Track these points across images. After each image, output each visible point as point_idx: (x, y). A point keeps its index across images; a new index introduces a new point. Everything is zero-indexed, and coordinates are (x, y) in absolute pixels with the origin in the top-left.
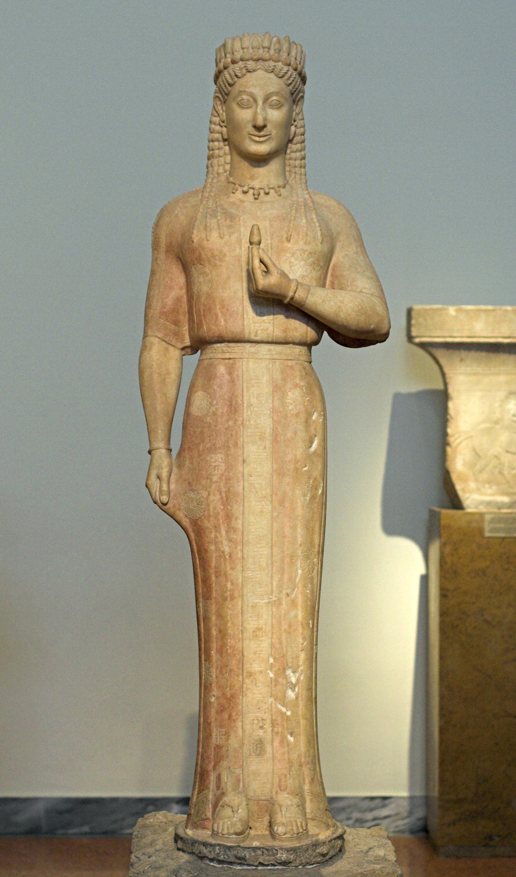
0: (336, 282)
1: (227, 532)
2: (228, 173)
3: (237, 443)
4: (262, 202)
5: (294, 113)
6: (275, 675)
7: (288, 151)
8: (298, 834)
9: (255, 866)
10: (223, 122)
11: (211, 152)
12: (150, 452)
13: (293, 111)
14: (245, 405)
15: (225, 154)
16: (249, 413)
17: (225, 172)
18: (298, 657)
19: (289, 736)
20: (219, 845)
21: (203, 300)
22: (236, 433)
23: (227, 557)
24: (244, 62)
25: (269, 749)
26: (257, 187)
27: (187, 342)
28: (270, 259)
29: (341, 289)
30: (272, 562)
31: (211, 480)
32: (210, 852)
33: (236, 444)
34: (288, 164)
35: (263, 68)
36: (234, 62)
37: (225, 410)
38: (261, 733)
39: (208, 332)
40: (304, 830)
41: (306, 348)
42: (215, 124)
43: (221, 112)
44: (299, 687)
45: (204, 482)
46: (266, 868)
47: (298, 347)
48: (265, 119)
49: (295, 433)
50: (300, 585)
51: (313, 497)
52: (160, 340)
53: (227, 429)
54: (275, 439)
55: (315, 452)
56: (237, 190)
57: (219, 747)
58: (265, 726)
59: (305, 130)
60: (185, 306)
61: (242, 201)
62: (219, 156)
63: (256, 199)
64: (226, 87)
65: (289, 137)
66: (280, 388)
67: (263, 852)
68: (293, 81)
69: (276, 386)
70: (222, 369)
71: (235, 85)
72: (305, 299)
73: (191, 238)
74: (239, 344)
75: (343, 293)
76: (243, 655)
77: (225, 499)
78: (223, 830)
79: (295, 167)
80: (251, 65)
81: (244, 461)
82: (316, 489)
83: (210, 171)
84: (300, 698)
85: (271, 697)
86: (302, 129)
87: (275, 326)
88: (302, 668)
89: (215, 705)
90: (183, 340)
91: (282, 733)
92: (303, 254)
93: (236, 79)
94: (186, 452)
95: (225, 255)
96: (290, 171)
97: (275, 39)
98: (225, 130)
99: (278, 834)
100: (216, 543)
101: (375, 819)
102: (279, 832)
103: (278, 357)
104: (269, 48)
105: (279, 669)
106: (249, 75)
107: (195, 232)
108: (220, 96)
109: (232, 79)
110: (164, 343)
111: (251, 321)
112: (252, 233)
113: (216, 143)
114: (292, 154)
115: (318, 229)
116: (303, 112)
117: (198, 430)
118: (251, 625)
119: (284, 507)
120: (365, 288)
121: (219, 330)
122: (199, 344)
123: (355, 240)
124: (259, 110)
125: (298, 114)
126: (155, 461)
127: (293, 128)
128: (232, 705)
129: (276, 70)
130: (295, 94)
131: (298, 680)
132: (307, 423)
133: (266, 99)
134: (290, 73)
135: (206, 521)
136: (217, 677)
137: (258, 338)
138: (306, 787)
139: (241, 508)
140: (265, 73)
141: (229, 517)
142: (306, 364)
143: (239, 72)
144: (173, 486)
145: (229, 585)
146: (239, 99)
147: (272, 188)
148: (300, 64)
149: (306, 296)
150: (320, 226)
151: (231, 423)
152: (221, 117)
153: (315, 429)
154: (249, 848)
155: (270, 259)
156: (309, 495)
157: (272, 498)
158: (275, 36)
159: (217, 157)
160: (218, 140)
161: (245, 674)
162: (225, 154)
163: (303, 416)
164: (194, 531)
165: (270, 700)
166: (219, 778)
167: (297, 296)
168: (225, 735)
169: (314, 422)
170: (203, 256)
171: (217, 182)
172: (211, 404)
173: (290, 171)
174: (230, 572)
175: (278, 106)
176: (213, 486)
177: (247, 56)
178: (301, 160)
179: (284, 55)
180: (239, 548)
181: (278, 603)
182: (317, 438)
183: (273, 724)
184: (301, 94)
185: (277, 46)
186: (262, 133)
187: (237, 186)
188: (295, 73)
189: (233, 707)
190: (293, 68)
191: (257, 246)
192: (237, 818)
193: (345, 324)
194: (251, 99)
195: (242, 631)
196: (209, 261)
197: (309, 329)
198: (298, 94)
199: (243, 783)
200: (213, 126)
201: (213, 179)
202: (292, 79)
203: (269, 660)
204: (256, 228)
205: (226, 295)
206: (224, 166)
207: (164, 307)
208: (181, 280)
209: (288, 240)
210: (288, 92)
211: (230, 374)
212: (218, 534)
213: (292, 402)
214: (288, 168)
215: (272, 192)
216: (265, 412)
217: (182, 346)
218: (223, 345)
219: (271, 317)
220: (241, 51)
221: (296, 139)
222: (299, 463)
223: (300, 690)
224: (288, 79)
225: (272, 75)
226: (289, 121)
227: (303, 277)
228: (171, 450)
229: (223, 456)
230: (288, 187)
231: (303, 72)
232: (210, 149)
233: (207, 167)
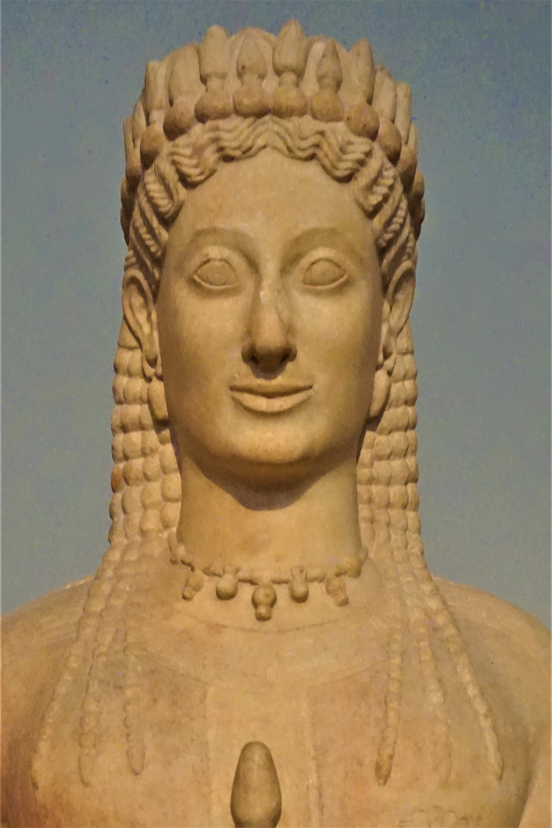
2: (174, 529)
5: (384, 329)
24: (209, 124)
34: (365, 497)
35: (280, 144)
43: (146, 329)
48: (289, 329)
64: (151, 230)
65: (369, 411)
71: (182, 217)
80: (235, 132)
83: (119, 527)
86: (408, 384)
93: (182, 193)
104: (300, 74)
108: (140, 276)
109: (171, 196)
114: (376, 464)
125: (396, 333)
127: (381, 378)
129: (325, 146)
143: (194, 162)
152: (146, 346)
171: (139, 560)
173: (372, 521)
177: (218, 104)
179: (352, 99)
184: (406, 265)
185: (328, 66)
188: (390, 173)
200: (123, 381)
201: (125, 551)
202: (381, 190)
206: (162, 510)
210: (370, 240)
221: (392, 415)
224: (370, 188)
225: (312, 170)
231: (417, 178)
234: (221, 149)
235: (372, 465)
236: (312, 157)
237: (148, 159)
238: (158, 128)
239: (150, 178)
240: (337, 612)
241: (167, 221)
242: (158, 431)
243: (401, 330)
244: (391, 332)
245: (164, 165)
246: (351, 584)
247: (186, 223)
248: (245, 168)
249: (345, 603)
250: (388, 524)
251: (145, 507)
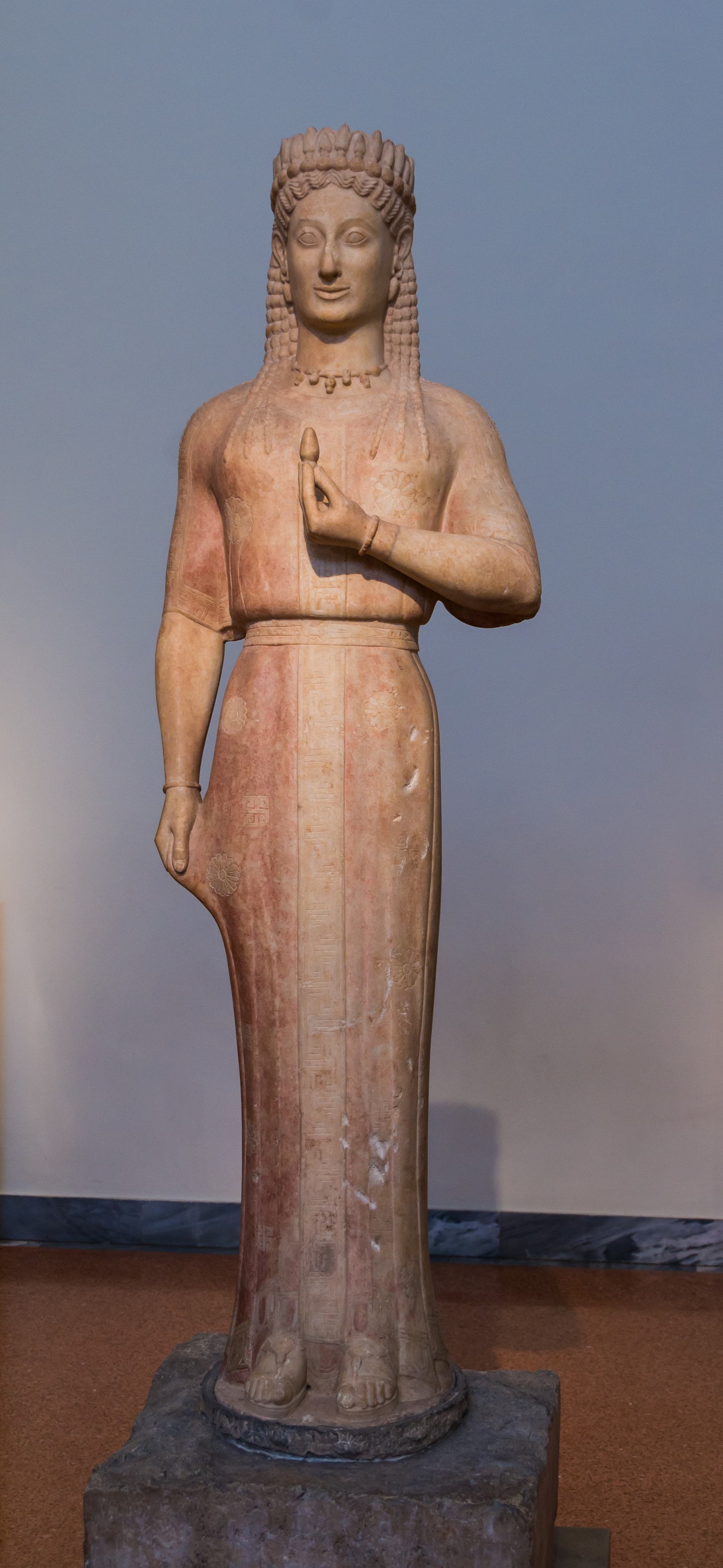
0: (456, 523)
1: (273, 918)
3: (288, 778)
4: (338, 398)
5: (395, 258)
6: (351, 1146)
7: (388, 319)
8: (374, 1406)
9: (301, 1456)
10: (285, 275)
11: (271, 325)
12: (165, 791)
13: (392, 255)
14: (300, 718)
15: (291, 327)
16: (307, 731)
17: (291, 354)
18: (388, 1117)
19: (373, 1243)
20: (249, 1418)
21: (239, 552)
22: (287, 763)
23: (274, 958)
24: (306, 173)
25: (340, 1262)
26: (331, 374)
27: (228, 621)
28: (332, 482)
29: (464, 533)
30: (345, 967)
31: (248, 835)
33: (286, 780)
36: (291, 174)
37: (270, 727)
38: (328, 1236)
39: (246, 602)
40: (385, 1399)
41: (402, 627)
42: (274, 280)
43: (282, 259)
44: (390, 1165)
45: (236, 839)
46: (321, 1460)
47: (387, 625)
49: (381, 763)
50: (391, 1004)
51: (411, 865)
52: (184, 617)
53: (272, 756)
54: (349, 772)
55: (414, 793)
56: (301, 380)
57: (264, 1255)
58: (335, 1226)
59: (416, 287)
60: (222, 563)
61: (308, 397)
62: (283, 331)
63: (329, 393)
64: (282, 216)
66: (356, 692)
67: (313, 1436)
68: (387, 202)
69: (351, 687)
70: (265, 661)
72: (390, 547)
73: (223, 454)
74: (294, 622)
75: (457, 538)
76: (300, 1112)
77: (269, 865)
78: (256, 1393)
79: (400, 344)
80: (316, 177)
81: (299, 807)
82: (417, 851)
84: (392, 1183)
85: (345, 1179)
86: (411, 284)
87: (349, 593)
89: (261, 1188)
90: (222, 617)
91: (361, 1237)
92: (395, 478)
93: (295, 202)
94: (214, 792)
95: (273, 480)
96: (391, 351)
97: (356, 136)
98: (287, 287)
99: (341, 1405)
100: (256, 936)
101: (690, 1248)
102: (343, 1402)
103: (354, 641)
104: (346, 150)
105: (358, 1137)
106: (313, 193)
107: (229, 445)
109: (290, 203)
110: (192, 622)
111: (311, 584)
112: (303, 442)
113: (277, 310)
114: (394, 323)
115: (424, 437)
116: (411, 257)
117: (230, 757)
118: (313, 1065)
119: (363, 880)
120: (499, 531)
121: (261, 598)
122: (241, 624)
123: (489, 456)
124: (327, 249)
126: (168, 805)
127: (394, 282)
128: (284, 1190)
130: (394, 225)
131: (389, 1154)
132: (399, 746)
133: (340, 232)
134: (379, 189)
135: (240, 901)
137: (322, 612)
138: (401, 1325)
139: (296, 880)
140: (339, 189)
141: (275, 894)
142: (404, 654)
144: (192, 847)
145: (277, 1002)
146: (300, 232)
147: (354, 376)
148: (401, 175)
149: (391, 542)
150: (427, 432)
151: (278, 746)
153: (414, 757)
154: (293, 1427)
155: (332, 482)
156: (404, 862)
157: (344, 867)
158: (358, 131)
159: (278, 332)
160: (279, 305)
161: (304, 1142)
162: (291, 327)
163: (393, 736)
164: (225, 916)
165: (344, 1185)
167: (376, 541)
168: (272, 1237)
169: (412, 745)
170: (240, 483)
172: (249, 716)
174: (278, 981)
175: (362, 242)
176: (252, 845)
177: (309, 165)
178: (411, 333)
179: (370, 160)
180: (293, 943)
181: (355, 1032)
182: (417, 771)
185: (359, 146)
186: (334, 286)
187: (302, 373)
188: (388, 190)
190: (385, 181)
191: (312, 463)
192: (280, 1375)
193: (460, 587)
194: (316, 232)
195: (299, 1074)
196: (248, 491)
197: (405, 596)
198: (399, 225)
199: (299, 1314)
200: (272, 283)
202: (384, 199)
204: (309, 433)
205: (273, 543)
207: (189, 565)
208: (213, 522)
209: (373, 455)
211: (280, 669)
212: (259, 922)
213: (375, 713)
214: (387, 346)
215: (355, 381)
216: (333, 729)
217: (219, 627)
218: (270, 623)
219: (342, 577)
220: (303, 156)
221: (400, 300)
222: (387, 811)
223: (393, 1170)
224: (377, 199)
225: (351, 193)
226: (382, 271)
227: (396, 514)
228: (199, 789)
229: (266, 799)
230: (384, 374)
232: (270, 320)
233: (266, 350)
234: (310, 184)
235: (392, 324)
236: (350, 187)
237: (281, 185)
238: (285, 172)
239: (281, 193)
240: (364, 390)
241: (290, 213)
242: (288, 308)
243: (406, 258)
244: (399, 259)
245: (287, 189)
246: (373, 379)
247: (298, 215)
248: (322, 192)
249: (369, 387)
250: (400, 353)
251: (281, 345)
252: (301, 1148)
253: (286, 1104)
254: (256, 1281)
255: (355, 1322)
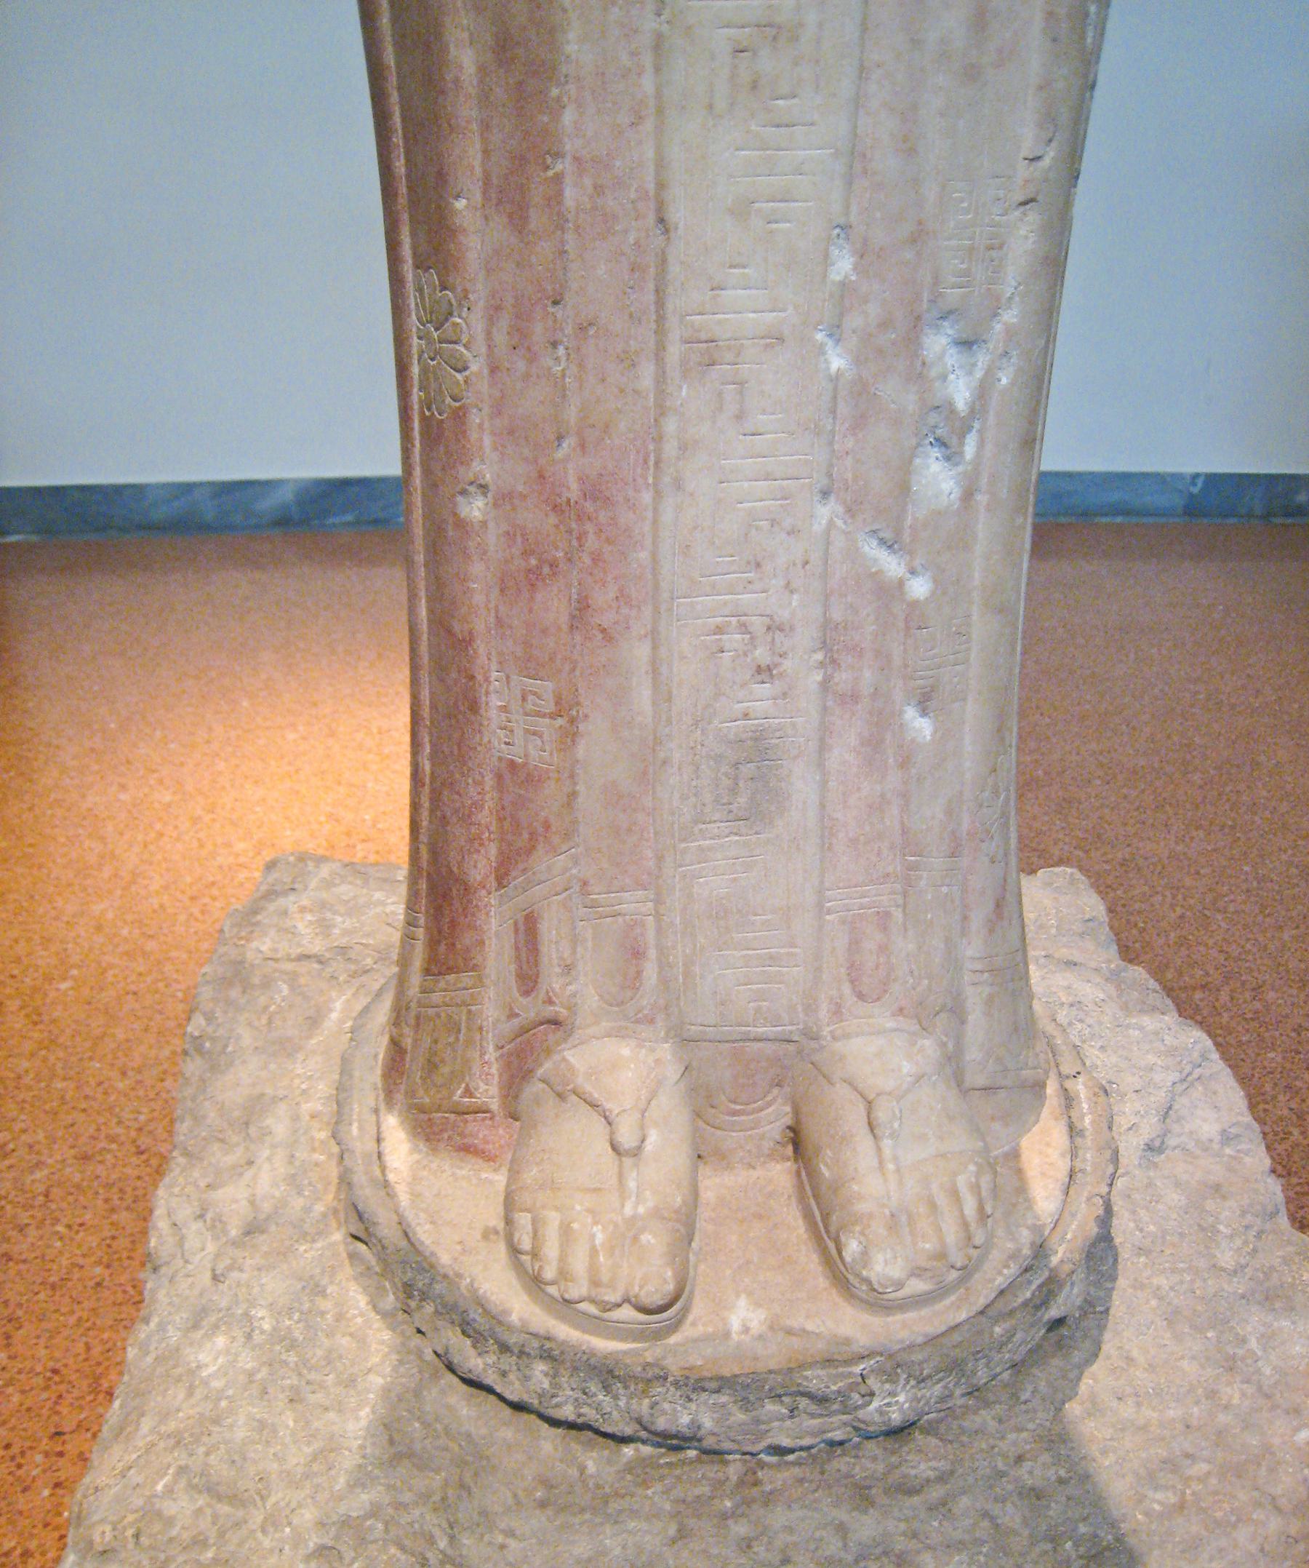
6: (858, 361)
19: (910, 713)
25: (802, 785)
32: (504, 1374)
57: (516, 775)
58: (787, 664)
85: (825, 494)
88: (1010, 316)
91: (876, 694)
105: (885, 325)
128: (591, 542)
131: (982, 392)
136: (494, 370)
161: (674, 351)
166: (528, 929)
168: (553, 716)
183: (833, 643)
189: (597, 559)
195: (659, 44)
199: (663, 965)
203: (826, 259)
223: (989, 447)
252: (661, 378)
253: (599, 189)
254: (493, 850)
255: (854, 973)
